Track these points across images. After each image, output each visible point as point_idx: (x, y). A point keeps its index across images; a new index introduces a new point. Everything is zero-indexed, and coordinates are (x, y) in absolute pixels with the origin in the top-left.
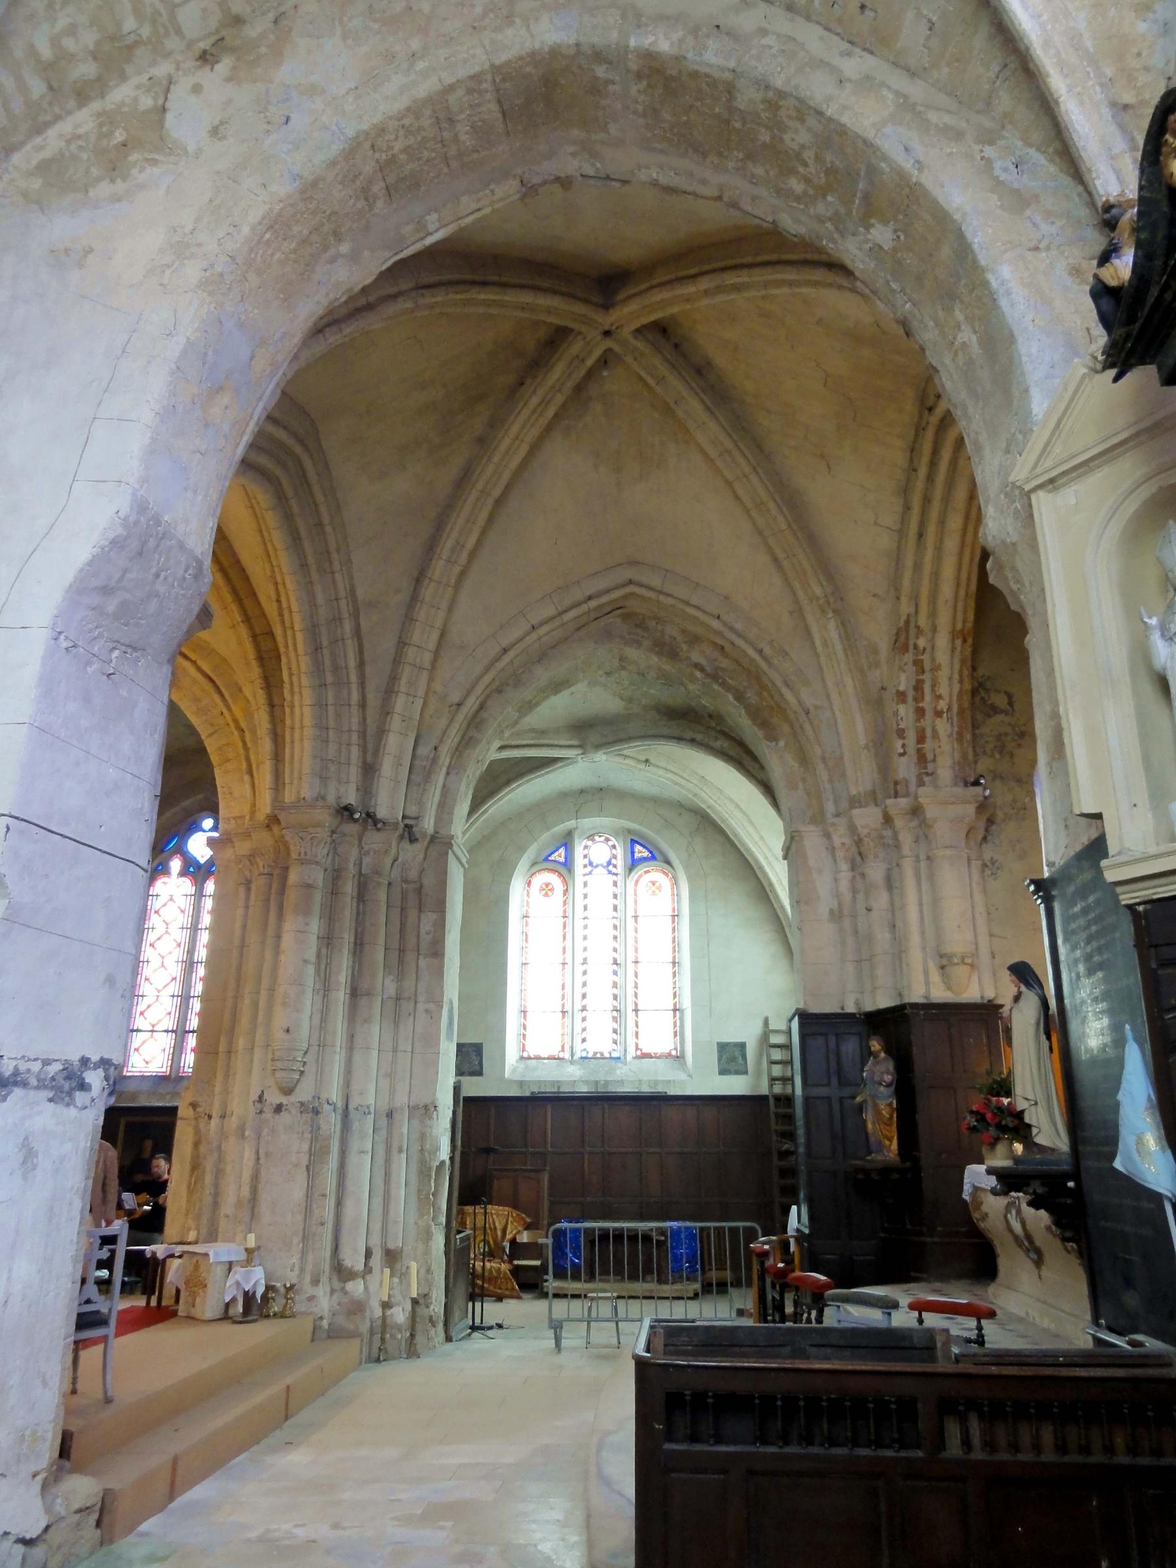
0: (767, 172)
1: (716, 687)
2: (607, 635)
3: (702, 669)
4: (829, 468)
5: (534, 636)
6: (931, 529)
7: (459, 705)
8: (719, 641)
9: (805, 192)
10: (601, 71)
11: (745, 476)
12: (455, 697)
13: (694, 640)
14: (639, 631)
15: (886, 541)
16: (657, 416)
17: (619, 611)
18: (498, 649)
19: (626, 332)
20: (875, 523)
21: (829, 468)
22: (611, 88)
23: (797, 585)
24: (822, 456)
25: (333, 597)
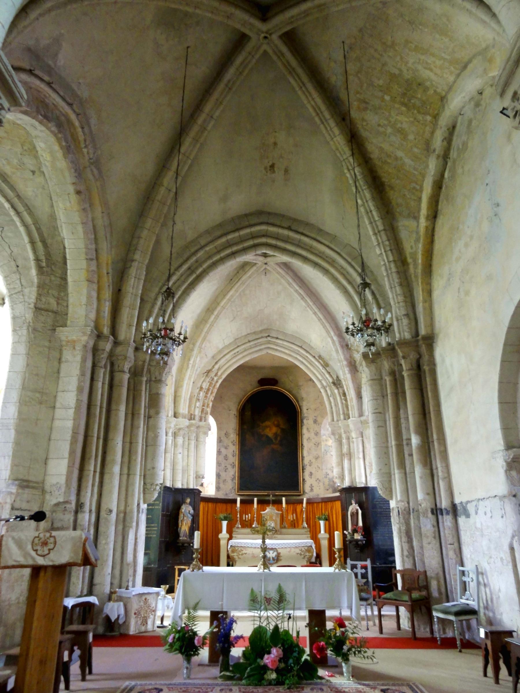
4: (232, 321)
6: (241, 356)
15: (221, 346)
19: (260, 263)
20: (223, 340)
21: (232, 321)
24: (234, 318)
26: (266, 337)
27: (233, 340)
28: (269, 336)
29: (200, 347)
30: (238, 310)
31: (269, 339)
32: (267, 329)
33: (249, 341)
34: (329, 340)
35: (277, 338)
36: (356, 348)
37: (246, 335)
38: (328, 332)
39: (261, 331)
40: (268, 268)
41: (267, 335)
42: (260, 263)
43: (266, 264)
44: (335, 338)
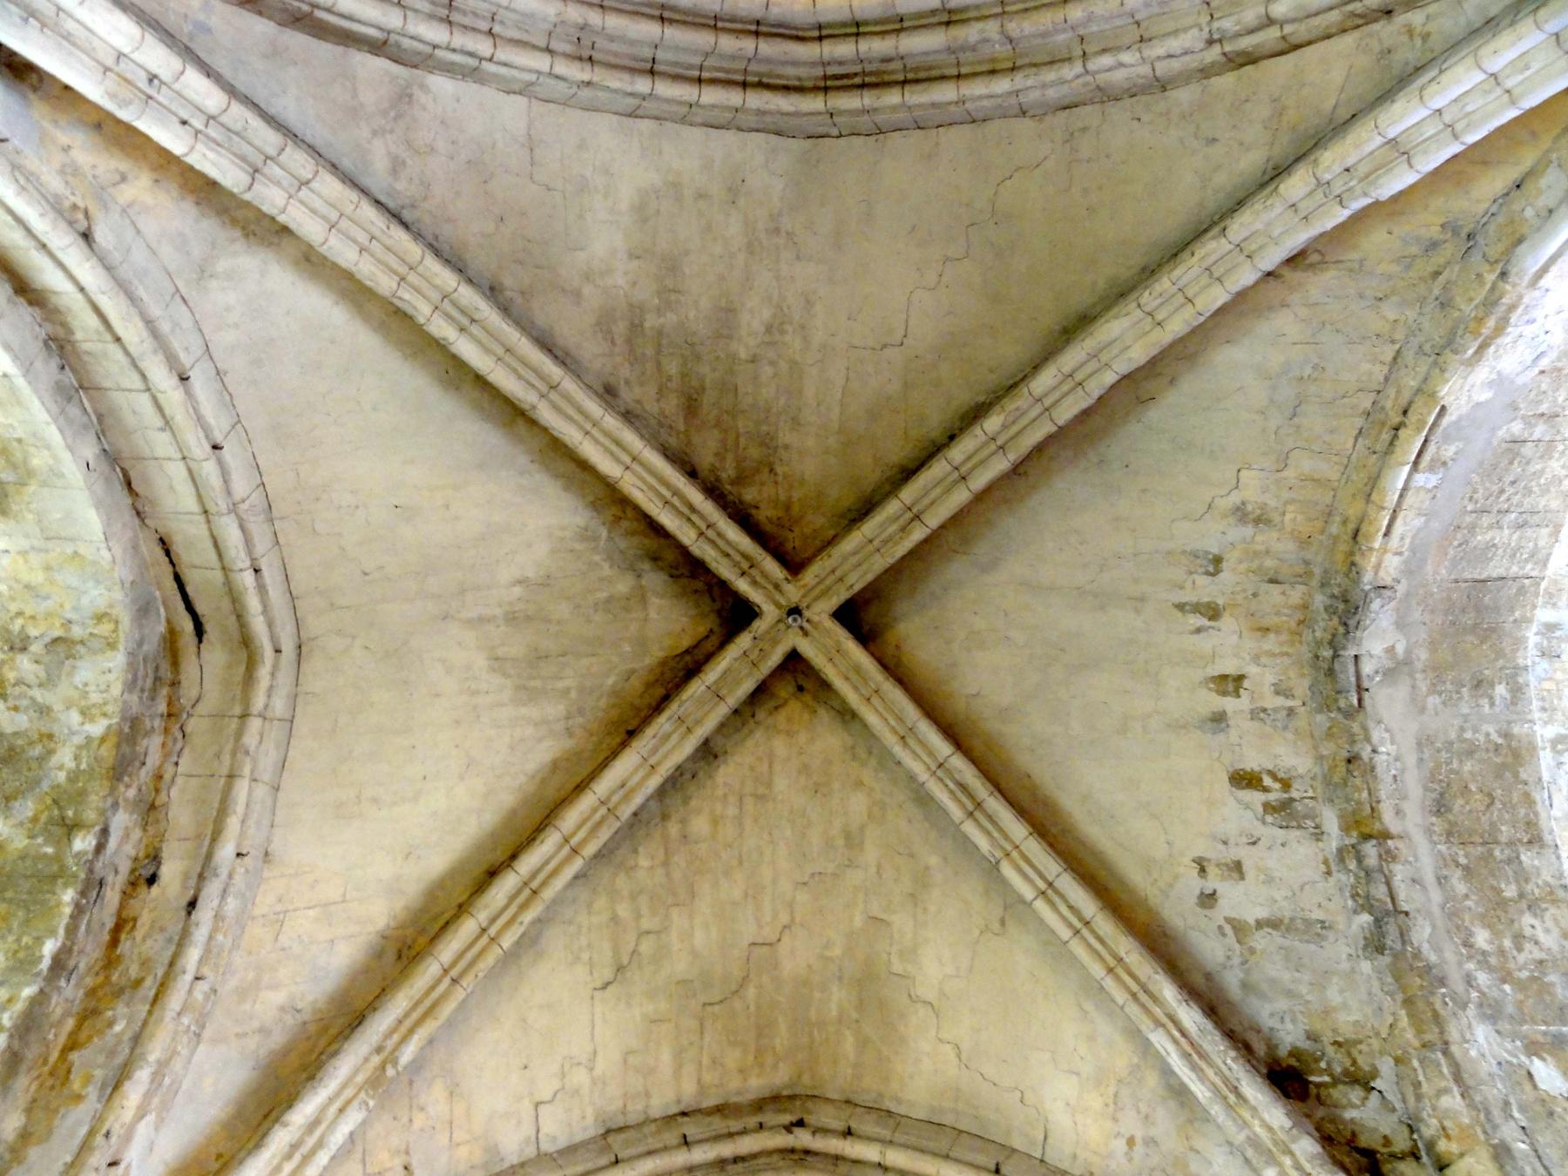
0: (1467, 896)
1: (68, 896)
2: (143, 611)
3: (100, 848)
4: (605, 986)
5: (199, 449)
7: (86, 236)
8: (171, 871)
9: (1484, 953)
10: (1501, 690)
11: (575, 851)
12: (101, 234)
13: (150, 810)
14: (149, 682)
16: (610, 681)
17: (188, 626)
18: (185, 359)
20: (537, 1105)
21: (605, 986)
22: (1485, 702)
23: (398, 1005)
24: (620, 969)
25: (497, 29)
26: (789, 1128)
27: (586, 1128)
28: (800, 1123)
29: (386, 1055)
30: (646, 924)
31: (803, 1139)
32: (792, 1098)
33: (686, 1142)
34: (1158, 1039)
35: (848, 1133)
36: (1340, 1062)
37: (672, 1117)
38: (1143, 994)
39: (759, 1105)
40: (807, 649)
41: (787, 1118)
42: (770, 612)
43: (795, 611)
44: (1191, 1017)
